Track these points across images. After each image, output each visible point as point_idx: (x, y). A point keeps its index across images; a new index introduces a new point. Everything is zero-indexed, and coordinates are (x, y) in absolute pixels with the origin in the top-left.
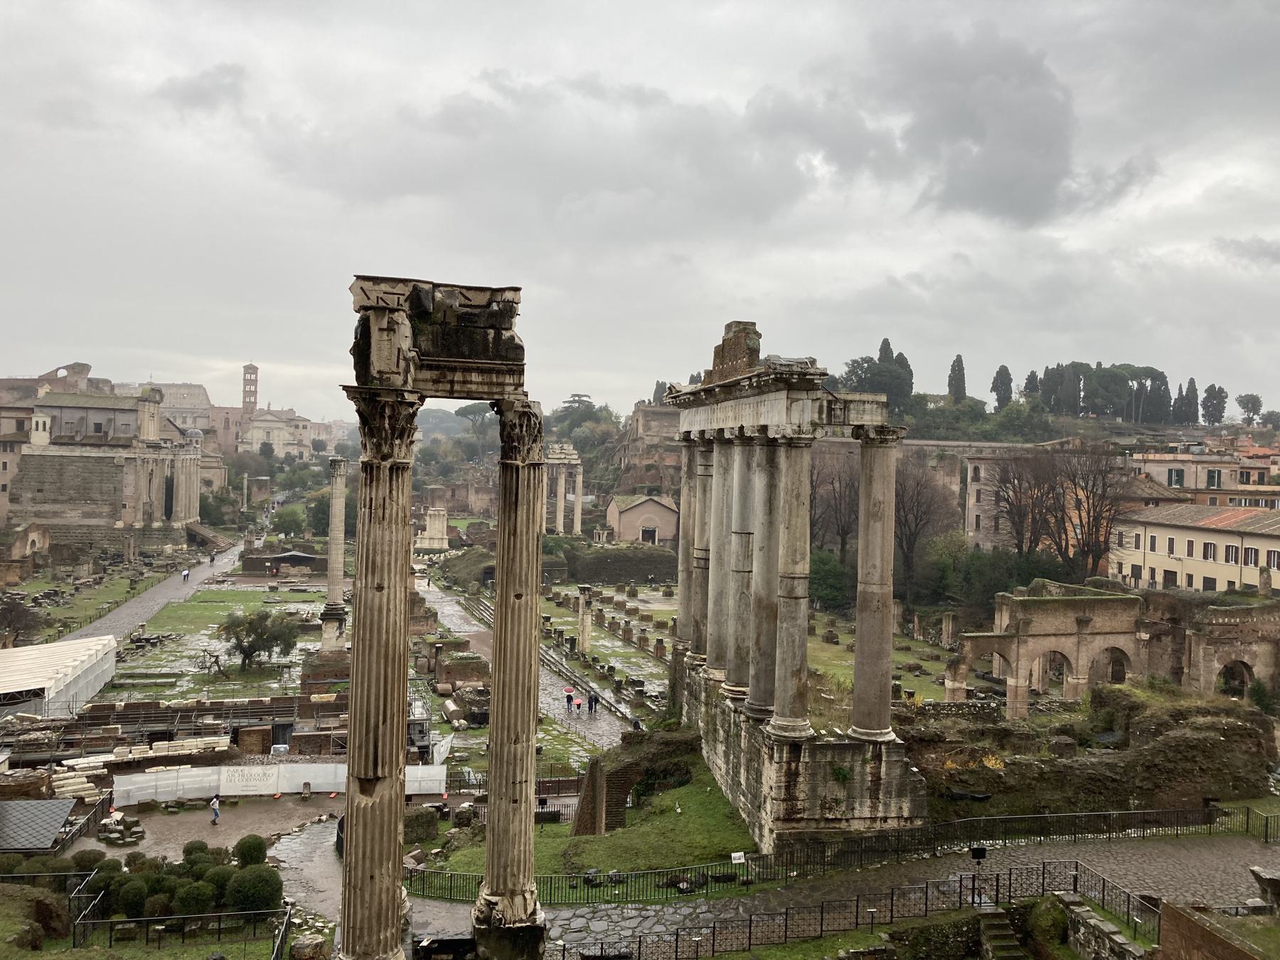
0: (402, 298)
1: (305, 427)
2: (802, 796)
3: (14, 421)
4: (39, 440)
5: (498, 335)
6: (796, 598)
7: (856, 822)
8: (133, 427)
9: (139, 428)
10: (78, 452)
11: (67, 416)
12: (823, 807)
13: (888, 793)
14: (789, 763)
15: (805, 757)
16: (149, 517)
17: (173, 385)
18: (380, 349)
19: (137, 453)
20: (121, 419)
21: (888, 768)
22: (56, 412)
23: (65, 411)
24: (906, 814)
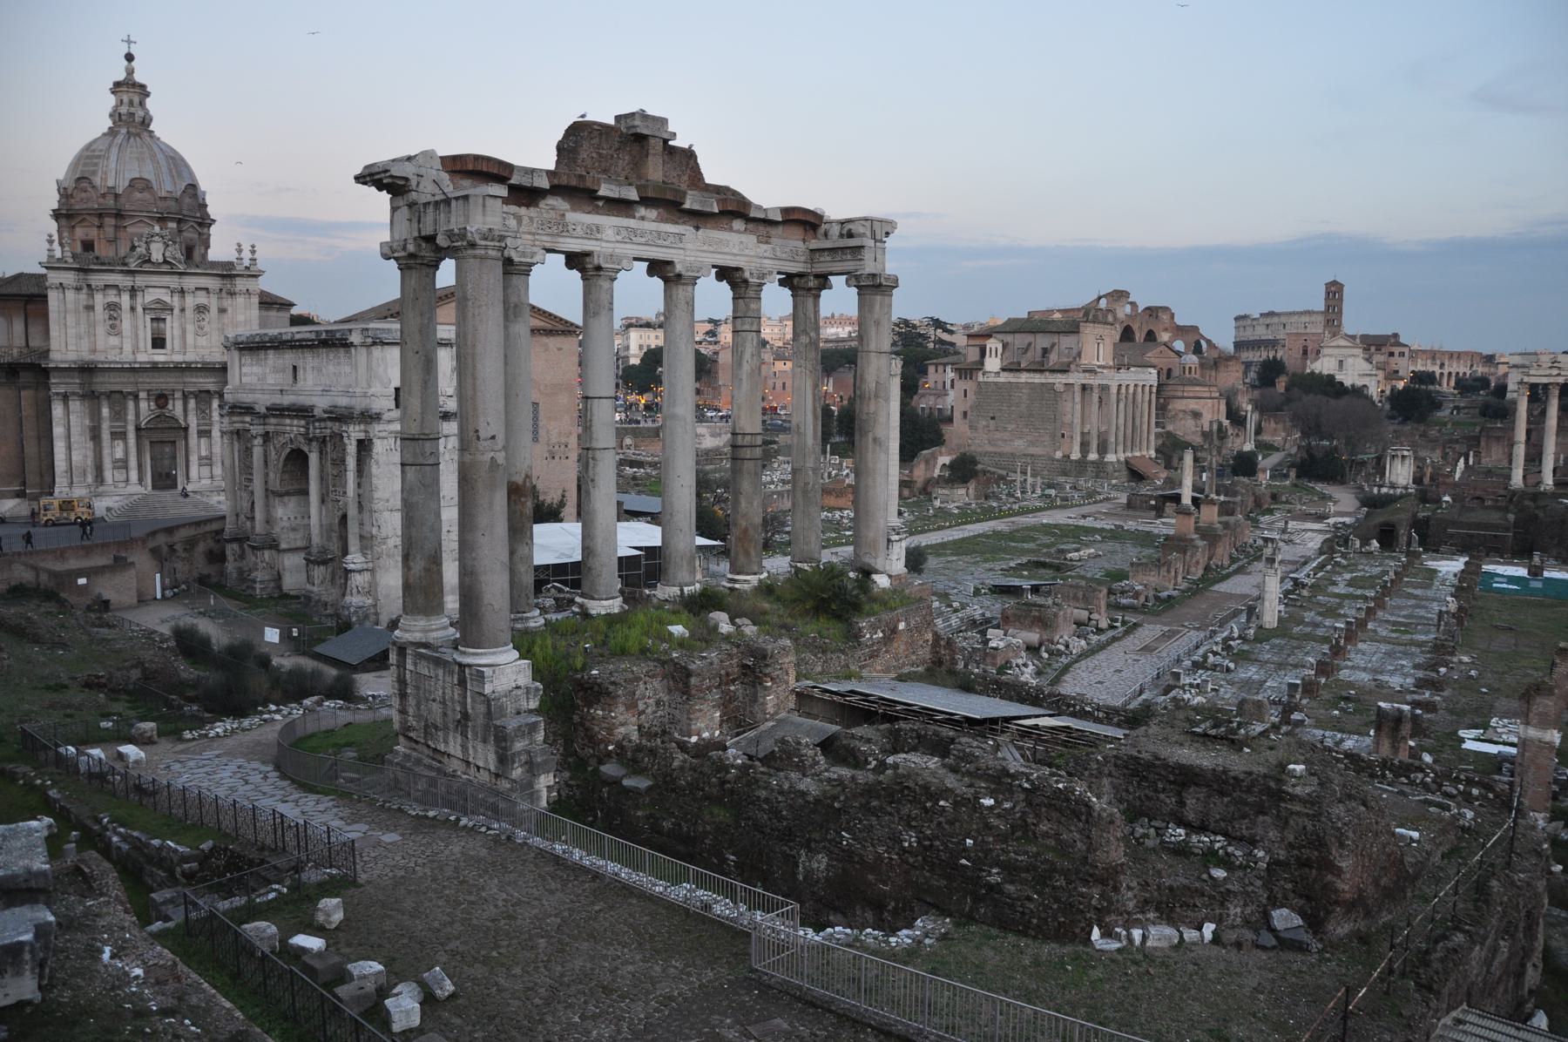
1: (1402, 354)
2: (411, 711)
3: (977, 350)
4: (992, 364)
7: (455, 761)
8: (1075, 352)
9: (1079, 354)
10: (1024, 378)
11: (1020, 340)
12: (426, 727)
13: (475, 734)
15: (409, 666)
16: (1085, 447)
17: (1294, 313)
19: (1076, 378)
20: (1066, 341)
21: (474, 701)
22: (1009, 338)
23: (1039, 336)
24: (492, 768)
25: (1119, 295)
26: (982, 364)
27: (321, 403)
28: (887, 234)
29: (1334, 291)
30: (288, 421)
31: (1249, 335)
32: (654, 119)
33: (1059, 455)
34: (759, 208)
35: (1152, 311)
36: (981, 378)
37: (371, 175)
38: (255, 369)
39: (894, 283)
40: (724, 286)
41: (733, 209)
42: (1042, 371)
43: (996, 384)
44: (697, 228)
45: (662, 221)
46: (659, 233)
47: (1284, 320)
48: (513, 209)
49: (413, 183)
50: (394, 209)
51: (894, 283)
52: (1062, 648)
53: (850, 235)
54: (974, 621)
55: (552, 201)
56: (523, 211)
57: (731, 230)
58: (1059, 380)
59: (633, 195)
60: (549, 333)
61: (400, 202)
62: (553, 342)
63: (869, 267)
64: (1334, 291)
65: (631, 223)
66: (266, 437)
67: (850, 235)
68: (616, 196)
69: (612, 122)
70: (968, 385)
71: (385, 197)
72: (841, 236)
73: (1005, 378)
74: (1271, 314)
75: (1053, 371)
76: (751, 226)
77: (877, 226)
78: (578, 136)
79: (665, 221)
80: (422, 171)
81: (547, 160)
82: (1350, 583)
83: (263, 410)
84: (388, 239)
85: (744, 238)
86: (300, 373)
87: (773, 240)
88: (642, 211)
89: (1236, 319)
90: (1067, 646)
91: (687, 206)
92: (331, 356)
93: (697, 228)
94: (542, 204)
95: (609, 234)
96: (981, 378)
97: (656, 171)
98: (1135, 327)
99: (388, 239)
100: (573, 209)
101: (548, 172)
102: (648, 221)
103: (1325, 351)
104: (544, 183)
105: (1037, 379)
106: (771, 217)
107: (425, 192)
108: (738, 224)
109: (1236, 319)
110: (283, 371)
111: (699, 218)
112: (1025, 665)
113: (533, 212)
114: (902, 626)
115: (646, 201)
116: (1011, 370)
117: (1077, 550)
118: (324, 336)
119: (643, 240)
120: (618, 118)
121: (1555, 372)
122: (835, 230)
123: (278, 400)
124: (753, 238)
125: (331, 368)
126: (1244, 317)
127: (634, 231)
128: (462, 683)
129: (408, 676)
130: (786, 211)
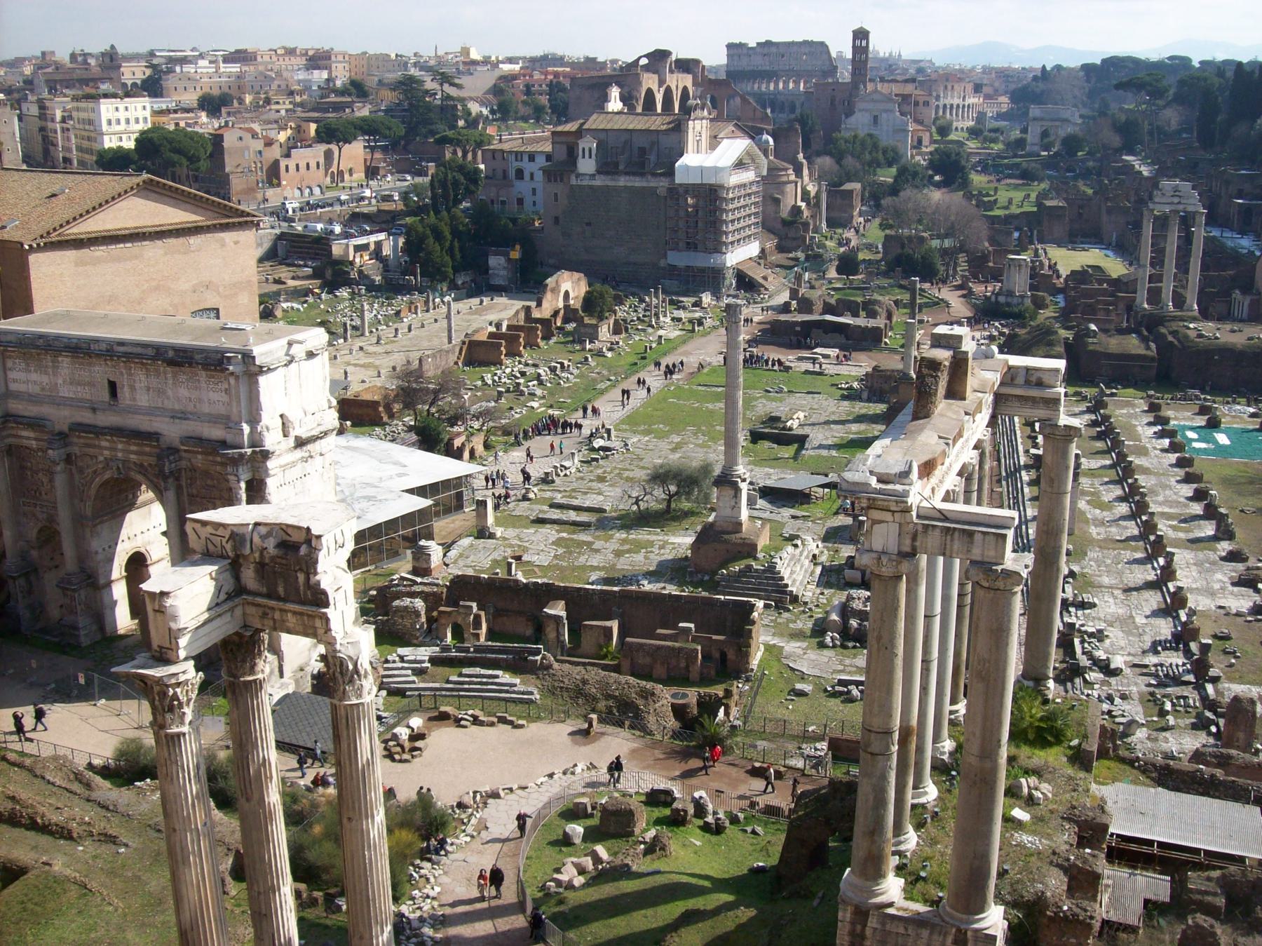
0: (224, 540)
3: (564, 148)
4: (587, 165)
5: (308, 579)
6: (872, 754)
10: (622, 181)
14: (853, 923)
15: (873, 922)
18: (157, 628)
26: (574, 164)
27: (172, 431)
30: (104, 444)
31: (744, 64)
36: (573, 181)
38: (34, 376)
42: (642, 175)
43: (591, 187)
47: (782, 50)
53: (1040, 384)
62: (228, 236)
66: (69, 459)
67: (1040, 384)
70: (559, 188)
73: (599, 182)
74: (768, 44)
83: (65, 428)
86: (125, 394)
89: (730, 46)
92: (183, 378)
96: (573, 181)
103: (860, 105)
105: (638, 182)
109: (730, 46)
110: (91, 384)
116: (607, 173)
118: (171, 354)
121: (1176, 200)
123: (86, 417)
125: (183, 392)
126: (741, 46)
129: (868, 932)
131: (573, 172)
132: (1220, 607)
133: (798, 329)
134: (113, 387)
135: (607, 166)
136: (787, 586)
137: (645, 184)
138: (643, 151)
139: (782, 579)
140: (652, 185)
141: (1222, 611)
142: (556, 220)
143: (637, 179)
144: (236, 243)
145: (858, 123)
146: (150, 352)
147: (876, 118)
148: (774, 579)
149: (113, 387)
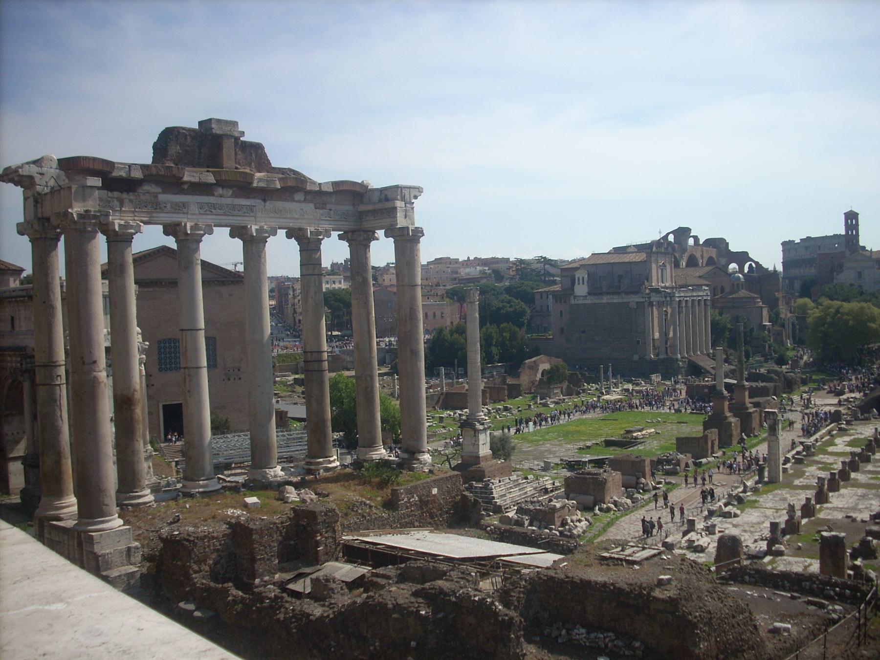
4: (581, 290)
10: (605, 299)
25: (682, 233)
28: (416, 197)
29: (851, 218)
30: (9, 359)
32: (227, 123)
33: (636, 357)
34: (314, 183)
35: (710, 242)
37: (7, 175)
39: (418, 233)
40: (293, 241)
41: (293, 185)
42: (619, 294)
43: (584, 305)
44: (265, 201)
45: (234, 195)
46: (234, 207)
48: (116, 194)
49: (38, 179)
50: (25, 199)
51: (418, 233)
52: (612, 506)
53: (387, 200)
54: (546, 489)
55: (146, 187)
56: (124, 196)
57: (293, 200)
58: (634, 299)
59: (210, 179)
60: (222, 283)
61: (30, 194)
63: (401, 222)
64: (851, 218)
65: (211, 199)
68: (197, 180)
69: (196, 126)
71: (19, 190)
72: (380, 201)
74: (809, 239)
75: (627, 293)
76: (309, 197)
77: (406, 192)
78: (169, 141)
79: (240, 197)
80: (45, 170)
81: (146, 157)
82: (850, 444)
84: (22, 220)
85: (303, 205)
87: (329, 206)
88: (220, 191)
90: (616, 506)
91: (255, 185)
93: (265, 201)
94: (140, 190)
95: (194, 208)
96: (573, 302)
97: (229, 160)
98: (698, 255)
99: (22, 220)
100: (164, 192)
101: (144, 167)
102: (225, 198)
104: (137, 174)
105: (616, 300)
106: (324, 189)
107: (44, 185)
108: (299, 196)
111: (265, 194)
112: (580, 521)
113: (132, 196)
114: (435, 491)
115: (220, 183)
116: (595, 294)
117: (640, 431)
119: (221, 212)
120: (200, 123)
122: (376, 198)
124: (312, 205)
127: (214, 206)
128: (80, 545)
130: (335, 184)
131: (572, 294)
132: (847, 517)
133: (706, 390)
134: (13, 318)
135: (595, 290)
136: (494, 498)
137: (620, 301)
138: (621, 277)
139: (492, 493)
140: (626, 300)
141: (850, 520)
142: (562, 330)
143: (615, 297)
144: (231, 295)
145: (846, 277)
146: (24, 293)
147: (860, 274)
148: (486, 493)
149: (13, 318)
